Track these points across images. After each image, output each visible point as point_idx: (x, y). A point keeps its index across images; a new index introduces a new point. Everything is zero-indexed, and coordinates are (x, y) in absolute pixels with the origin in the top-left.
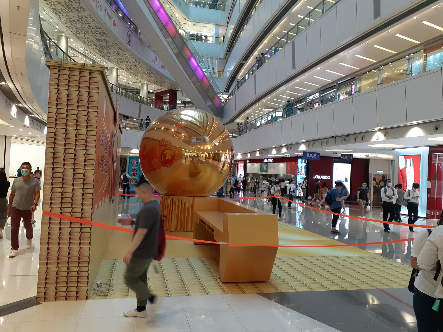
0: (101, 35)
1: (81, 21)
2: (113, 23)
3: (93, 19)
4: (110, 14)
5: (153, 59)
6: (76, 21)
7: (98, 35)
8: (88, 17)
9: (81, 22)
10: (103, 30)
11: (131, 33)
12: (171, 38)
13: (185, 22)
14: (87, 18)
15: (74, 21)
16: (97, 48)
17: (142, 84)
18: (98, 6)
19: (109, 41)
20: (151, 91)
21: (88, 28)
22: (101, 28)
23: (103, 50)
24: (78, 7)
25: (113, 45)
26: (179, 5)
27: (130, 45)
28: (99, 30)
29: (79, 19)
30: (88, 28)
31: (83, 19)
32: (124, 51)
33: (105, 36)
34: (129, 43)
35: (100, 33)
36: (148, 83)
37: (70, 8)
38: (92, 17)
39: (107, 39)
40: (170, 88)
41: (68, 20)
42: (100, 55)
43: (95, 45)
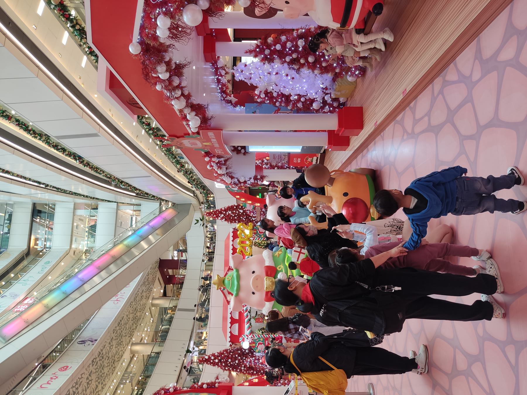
2: (63, 371)
5: (117, 300)
7: (80, 390)
12: (84, 284)
13: (72, 253)
16: (101, 382)
17: (153, 305)
20: (162, 291)
22: (69, 390)
23: (104, 373)
25: (95, 364)
26: (49, 265)
27: (96, 339)
33: (81, 381)
34: (92, 342)
35: (77, 389)
36: (151, 298)
39: (85, 376)
40: (157, 269)
42: (112, 374)
43: (97, 386)
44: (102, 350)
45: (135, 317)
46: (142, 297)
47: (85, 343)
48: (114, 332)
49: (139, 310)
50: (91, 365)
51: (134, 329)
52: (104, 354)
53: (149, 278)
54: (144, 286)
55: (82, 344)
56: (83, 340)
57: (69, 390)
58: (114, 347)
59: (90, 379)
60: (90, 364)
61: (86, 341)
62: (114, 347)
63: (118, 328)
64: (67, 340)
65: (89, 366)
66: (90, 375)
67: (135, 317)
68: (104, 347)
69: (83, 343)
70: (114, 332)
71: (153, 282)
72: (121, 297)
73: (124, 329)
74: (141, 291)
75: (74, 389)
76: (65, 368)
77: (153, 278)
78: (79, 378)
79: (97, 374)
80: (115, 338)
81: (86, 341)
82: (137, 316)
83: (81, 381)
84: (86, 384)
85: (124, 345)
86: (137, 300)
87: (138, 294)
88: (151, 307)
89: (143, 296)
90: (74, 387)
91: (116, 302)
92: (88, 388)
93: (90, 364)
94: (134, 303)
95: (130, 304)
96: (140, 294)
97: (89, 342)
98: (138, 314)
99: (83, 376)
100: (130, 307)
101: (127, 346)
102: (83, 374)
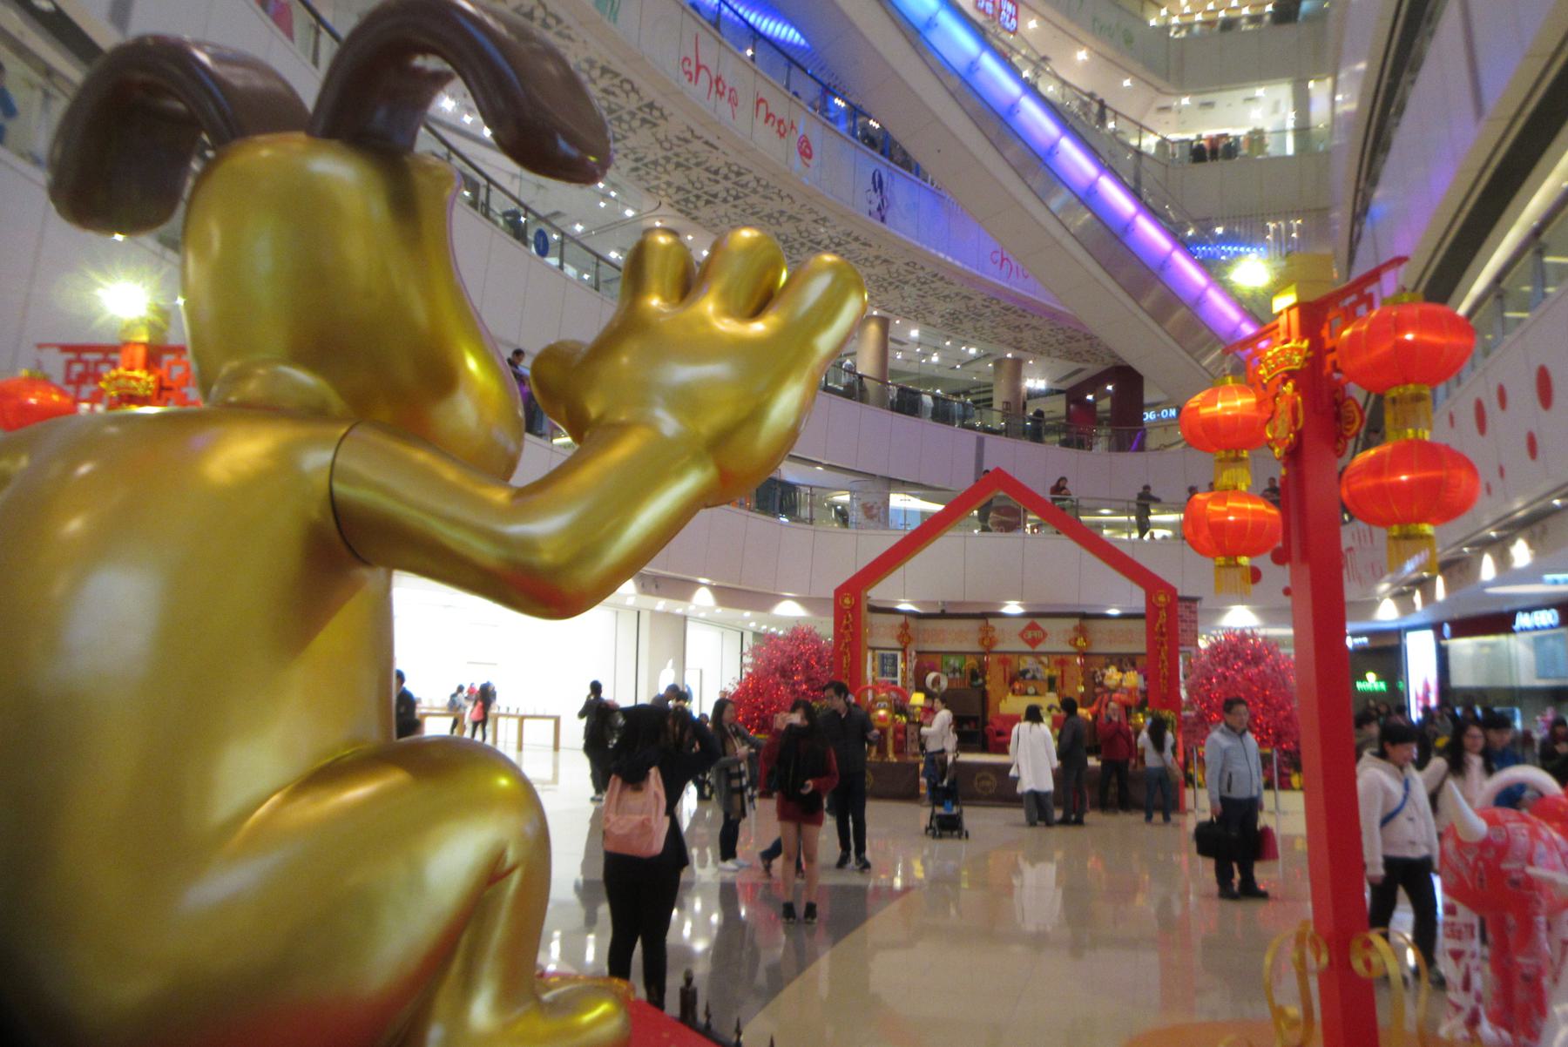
0: (766, 197)
1: (675, 159)
2: (800, 148)
3: (707, 143)
4: (779, 115)
5: (1003, 260)
6: (662, 161)
7: (754, 199)
8: (688, 135)
9: (678, 165)
10: (759, 175)
11: (890, 174)
14: (686, 141)
15: (655, 163)
18: (718, 91)
19: (799, 216)
21: (710, 179)
22: (750, 172)
24: (640, 109)
27: (888, 219)
28: (744, 179)
29: (665, 153)
30: (710, 179)
31: (676, 149)
32: (870, 246)
33: (774, 196)
34: (879, 209)
35: (755, 191)
36: (1020, 354)
37: (620, 119)
38: (696, 133)
41: (639, 164)
44: (856, 239)
45: (957, 318)
46: (1017, 330)
47: (876, 190)
48: (908, 264)
49: (979, 325)
50: (815, 217)
51: (925, 318)
52: (848, 246)
53: (1078, 341)
54: (1052, 330)
55: (874, 182)
56: (885, 185)
57: (750, 172)
58: (871, 271)
59: (783, 219)
60: (816, 213)
61: (881, 192)
62: (871, 271)
63: (921, 273)
64: (881, 144)
65: (811, 211)
66: (790, 217)
67: (957, 318)
68: (865, 244)
69: (875, 186)
70: (908, 264)
71: (1071, 355)
72: (1014, 269)
73: (920, 290)
74: (1034, 322)
75: (753, 184)
76: (808, 151)
77: (1079, 353)
78: (780, 191)
79: (797, 236)
80: (893, 269)
81: (881, 192)
82: (961, 322)
83: (774, 196)
84: (767, 210)
85: (878, 298)
86: (1005, 315)
87: (1025, 317)
88: (995, 358)
89: (1021, 331)
90: (758, 181)
91: (998, 257)
92: (761, 218)
93: (816, 213)
94: (996, 308)
95: (993, 299)
96: (1026, 321)
97: (879, 201)
98: (968, 325)
99: (787, 201)
100: (985, 300)
101: (878, 305)
102: (791, 198)
